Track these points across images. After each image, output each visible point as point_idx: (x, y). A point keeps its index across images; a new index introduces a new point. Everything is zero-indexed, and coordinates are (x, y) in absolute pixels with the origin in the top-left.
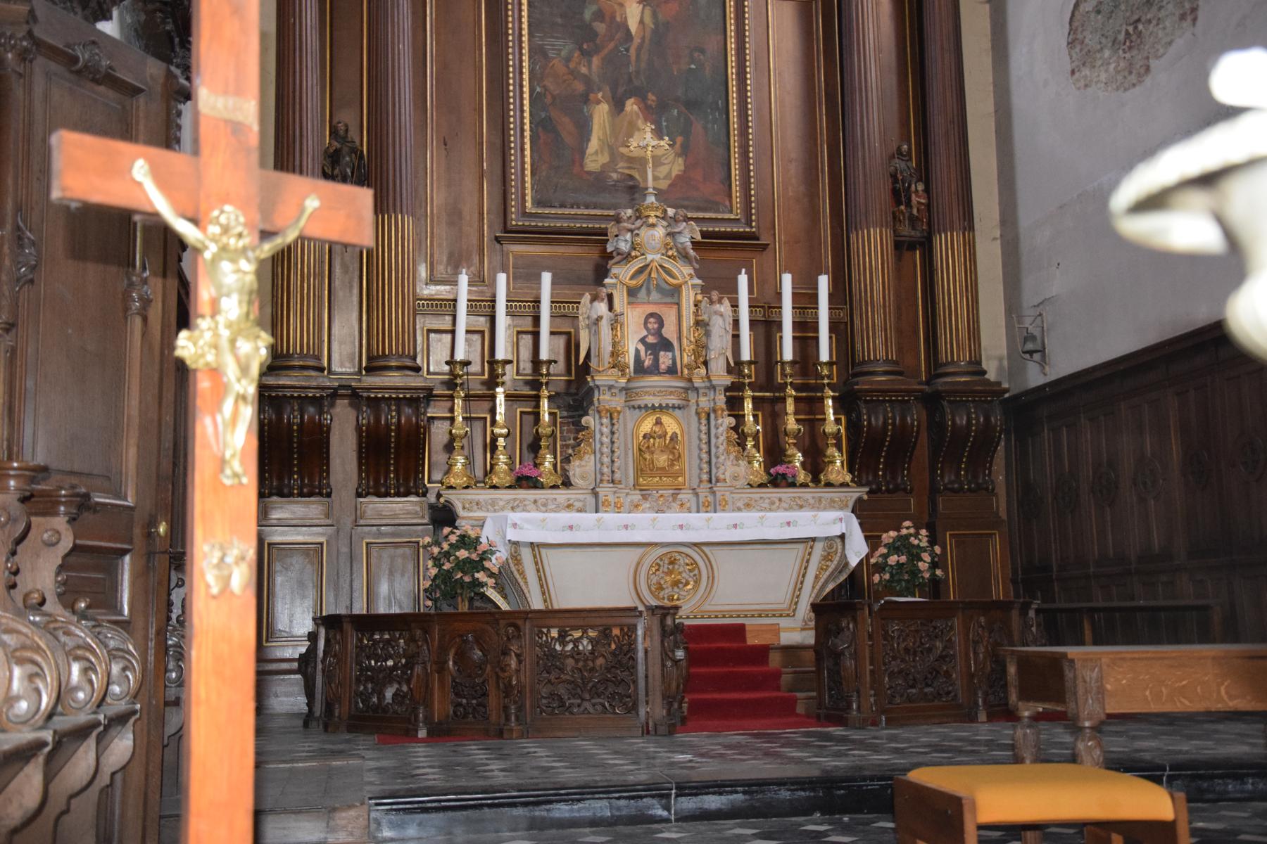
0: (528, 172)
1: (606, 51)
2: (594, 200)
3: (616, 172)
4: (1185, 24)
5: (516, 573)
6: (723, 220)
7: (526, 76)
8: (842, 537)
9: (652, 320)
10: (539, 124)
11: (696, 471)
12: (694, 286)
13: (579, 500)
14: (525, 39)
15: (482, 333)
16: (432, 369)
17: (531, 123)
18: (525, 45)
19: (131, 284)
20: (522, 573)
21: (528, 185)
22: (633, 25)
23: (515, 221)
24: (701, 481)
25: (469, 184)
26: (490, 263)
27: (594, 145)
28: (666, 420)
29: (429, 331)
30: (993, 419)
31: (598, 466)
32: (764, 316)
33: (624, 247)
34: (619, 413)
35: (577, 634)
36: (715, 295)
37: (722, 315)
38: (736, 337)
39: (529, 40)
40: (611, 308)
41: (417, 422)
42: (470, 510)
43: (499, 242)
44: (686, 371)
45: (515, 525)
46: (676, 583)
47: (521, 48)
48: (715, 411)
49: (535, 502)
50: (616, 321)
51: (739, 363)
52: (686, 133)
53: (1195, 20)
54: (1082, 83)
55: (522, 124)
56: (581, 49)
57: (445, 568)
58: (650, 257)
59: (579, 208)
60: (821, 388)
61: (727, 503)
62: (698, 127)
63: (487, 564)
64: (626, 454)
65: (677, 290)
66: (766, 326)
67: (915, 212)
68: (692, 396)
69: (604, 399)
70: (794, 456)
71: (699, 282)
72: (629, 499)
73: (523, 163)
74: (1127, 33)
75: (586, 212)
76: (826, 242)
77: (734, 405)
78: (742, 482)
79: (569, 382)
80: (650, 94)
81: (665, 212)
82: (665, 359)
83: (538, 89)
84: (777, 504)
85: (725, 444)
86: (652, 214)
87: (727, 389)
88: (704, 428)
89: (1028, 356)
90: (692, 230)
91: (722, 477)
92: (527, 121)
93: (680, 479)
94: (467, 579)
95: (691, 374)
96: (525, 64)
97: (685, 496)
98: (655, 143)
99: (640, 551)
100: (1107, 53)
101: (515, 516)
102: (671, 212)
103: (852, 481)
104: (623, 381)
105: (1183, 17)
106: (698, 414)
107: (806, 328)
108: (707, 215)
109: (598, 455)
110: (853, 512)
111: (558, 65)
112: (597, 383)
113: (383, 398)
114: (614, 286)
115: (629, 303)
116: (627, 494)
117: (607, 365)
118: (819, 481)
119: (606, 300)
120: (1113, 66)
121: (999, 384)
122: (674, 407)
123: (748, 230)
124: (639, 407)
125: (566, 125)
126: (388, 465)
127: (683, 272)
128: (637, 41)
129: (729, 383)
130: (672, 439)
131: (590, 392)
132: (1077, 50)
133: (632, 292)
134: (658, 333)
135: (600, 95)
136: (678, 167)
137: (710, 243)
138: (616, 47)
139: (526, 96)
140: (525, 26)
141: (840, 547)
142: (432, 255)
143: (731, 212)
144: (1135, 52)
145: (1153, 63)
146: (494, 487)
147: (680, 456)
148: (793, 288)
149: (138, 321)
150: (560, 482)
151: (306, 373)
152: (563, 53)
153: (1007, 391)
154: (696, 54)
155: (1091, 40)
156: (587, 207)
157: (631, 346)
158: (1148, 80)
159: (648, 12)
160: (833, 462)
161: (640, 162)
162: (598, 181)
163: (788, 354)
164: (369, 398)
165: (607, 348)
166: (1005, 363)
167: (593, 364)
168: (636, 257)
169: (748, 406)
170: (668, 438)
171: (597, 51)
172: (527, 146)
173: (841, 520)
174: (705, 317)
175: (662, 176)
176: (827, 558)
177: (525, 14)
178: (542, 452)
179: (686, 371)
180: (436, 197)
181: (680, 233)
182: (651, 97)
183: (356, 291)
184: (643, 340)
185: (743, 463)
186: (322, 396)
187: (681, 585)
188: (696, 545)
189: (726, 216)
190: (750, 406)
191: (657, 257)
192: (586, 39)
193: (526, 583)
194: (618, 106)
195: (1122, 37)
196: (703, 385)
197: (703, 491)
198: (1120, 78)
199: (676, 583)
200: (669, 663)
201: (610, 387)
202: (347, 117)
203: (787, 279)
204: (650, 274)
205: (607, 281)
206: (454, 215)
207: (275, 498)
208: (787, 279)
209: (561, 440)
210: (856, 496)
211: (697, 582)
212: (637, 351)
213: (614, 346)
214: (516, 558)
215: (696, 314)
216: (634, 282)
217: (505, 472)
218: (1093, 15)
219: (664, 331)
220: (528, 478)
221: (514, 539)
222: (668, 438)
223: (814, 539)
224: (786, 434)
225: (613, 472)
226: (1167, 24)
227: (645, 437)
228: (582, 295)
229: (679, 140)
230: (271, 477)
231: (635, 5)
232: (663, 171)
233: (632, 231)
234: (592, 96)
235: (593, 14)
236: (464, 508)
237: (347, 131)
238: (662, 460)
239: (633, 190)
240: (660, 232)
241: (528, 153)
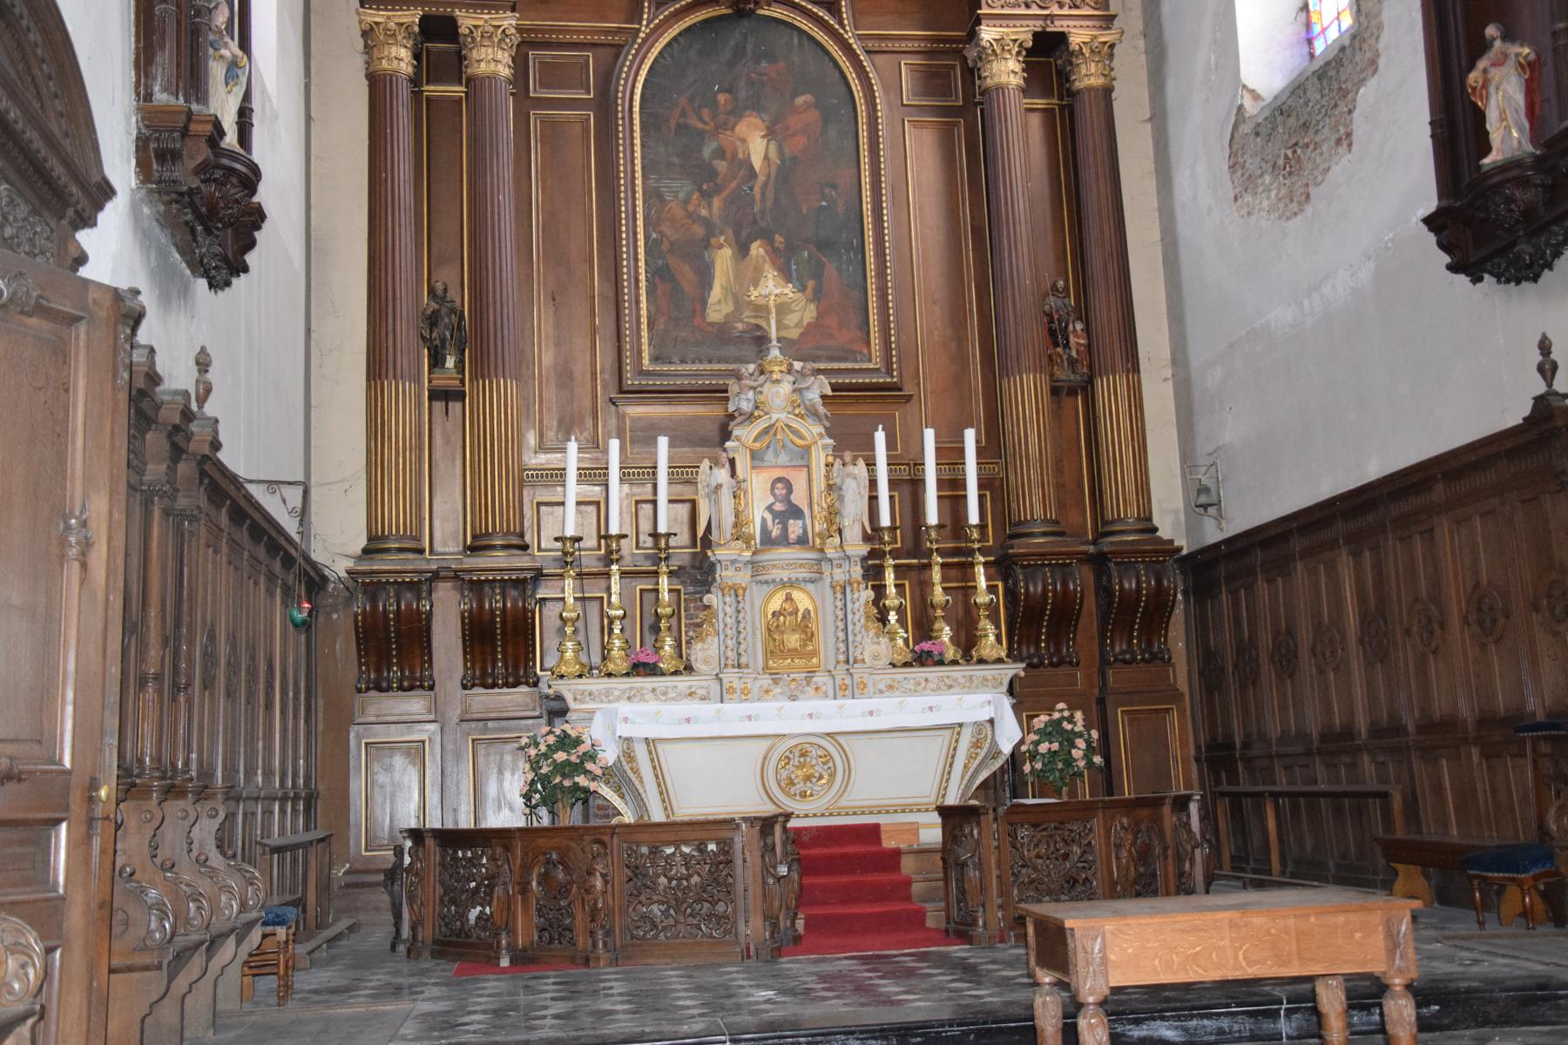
0: (644, 326)
1: (726, 193)
2: (718, 353)
3: (742, 321)
4: (1341, 150)
5: (629, 772)
6: (861, 370)
7: (640, 223)
8: (991, 721)
9: (779, 485)
10: (659, 274)
11: (832, 652)
12: (825, 447)
13: (702, 687)
14: (639, 182)
15: (598, 504)
16: (543, 546)
17: (646, 272)
18: (639, 189)
19: (68, 528)
20: (636, 772)
21: (645, 340)
22: (757, 162)
23: (630, 380)
24: (838, 662)
25: (580, 342)
26: (604, 426)
27: (716, 293)
28: (797, 595)
29: (539, 504)
30: (1166, 583)
31: (722, 648)
32: (910, 474)
33: (746, 406)
34: (745, 589)
35: (669, 850)
36: (848, 456)
37: (855, 478)
38: (873, 499)
39: (643, 183)
40: (733, 474)
41: (524, 606)
42: (582, 702)
43: (614, 403)
44: (818, 541)
45: (626, 720)
46: (808, 778)
47: (634, 192)
48: (850, 584)
49: (654, 690)
50: (739, 488)
51: (876, 528)
52: (818, 275)
53: (1350, 145)
54: (1245, 211)
55: (637, 274)
56: (700, 190)
57: (542, 771)
58: (775, 417)
59: (701, 362)
60: (971, 552)
61: (865, 686)
62: (831, 269)
63: (589, 766)
64: (754, 633)
65: (807, 450)
66: (908, 485)
67: (1074, 354)
68: (826, 567)
69: (725, 575)
70: (941, 630)
71: (830, 441)
72: (758, 684)
73: (639, 317)
74: (1286, 157)
75: (709, 367)
76: (976, 390)
77: (873, 574)
78: (884, 661)
79: (694, 555)
80: (777, 236)
81: (791, 365)
82: (795, 528)
83: (654, 235)
84: (923, 684)
85: (862, 620)
86: (776, 369)
87: (864, 559)
88: (839, 604)
89: (1201, 510)
90: (821, 385)
91: (860, 657)
92: (642, 270)
93: (814, 660)
94: (567, 783)
95: (823, 543)
96: (640, 209)
97: (821, 679)
98: (778, 291)
99: (765, 744)
100: (1267, 179)
101: (624, 708)
102: (798, 365)
103: (1008, 656)
104: (748, 554)
105: (1338, 142)
106: (833, 587)
107: (952, 488)
108: (843, 366)
109: (722, 637)
110: (1011, 691)
111: (675, 208)
112: (718, 557)
113: (487, 580)
114: (735, 450)
115: (753, 468)
116: (755, 679)
117: (729, 537)
118: (972, 657)
119: (727, 465)
120: (1273, 193)
121: (1172, 542)
122: (804, 580)
123: (889, 380)
124: (767, 582)
125: (686, 274)
126: (494, 653)
127: (813, 430)
128: (762, 178)
129: (865, 553)
130: (804, 617)
131: (712, 566)
132: (1239, 174)
133: (755, 456)
134: (787, 499)
135: (722, 239)
136: (810, 313)
137: (841, 394)
138: (739, 187)
139: (641, 243)
140: (638, 168)
141: (989, 733)
142: (541, 421)
143: (870, 361)
144: (1294, 179)
145: (1313, 191)
146: (609, 675)
147: (812, 635)
148: (936, 442)
149: (76, 565)
150: (682, 667)
151: (402, 556)
152: (681, 195)
153: (1180, 549)
154: (827, 191)
155: (1252, 164)
156: (710, 362)
157: (758, 514)
158: (1309, 209)
159: (773, 147)
160: (986, 636)
161: (761, 310)
162: (722, 335)
163: (932, 517)
164: (471, 581)
165: (728, 519)
166: (1182, 517)
167: (714, 537)
168: (760, 417)
169: (890, 577)
170: (800, 615)
171: (718, 190)
172: (643, 298)
173: (989, 702)
174: (837, 481)
175: (792, 325)
176: (977, 744)
177: (638, 155)
178: (662, 634)
179: (818, 541)
180: (547, 357)
181: (808, 388)
182: (779, 239)
183: (459, 463)
184: (770, 508)
185: (884, 640)
186: (420, 581)
187: (814, 780)
188: (828, 734)
189: (865, 366)
190: (892, 576)
191: (783, 416)
192: (705, 179)
193: (642, 782)
194: (743, 250)
195: (1281, 162)
196: (837, 555)
197: (840, 673)
198: (1281, 206)
199: (808, 778)
200: (771, 881)
201: (733, 562)
202: (447, 276)
203: (929, 435)
204: (775, 434)
205: (728, 444)
206: (565, 376)
207: (373, 693)
208: (929, 435)
209: (686, 618)
210: (1011, 673)
211: (832, 775)
212: (764, 520)
213: (737, 516)
214: (629, 755)
215: (827, 477)
216: (758, 445)
217: (621, 658)
218: (1252, 137)
219: (793, 497)
220: (645, 665)
221: (625, 735)
222: (800, 615)
223: (961, 725)
224: (933, 606)
225: (739, 655)
226: (1325, 148)
227: (774, 614)
228: (700, 460)
229: (811, 284)
230: (368, 670)
231: (759, 140)
232: (792, 319)
233: (754, 388)
234: (713, 241)
235: (713, 152)
236: (575, 699)
237: (445, 290)
238: (793, 640)
239: (760, 341)
240: (786, 388)
241: (644, 305)
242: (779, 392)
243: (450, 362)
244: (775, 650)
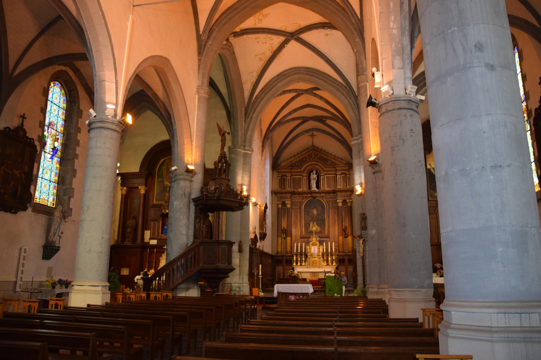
10: (305, 225)
22: (315, 214)
23: (302, 237)
33: (311, 240)
52: (321, 226)
69: (308, 257)
125: (308, 225)
194: (313, 223)
242: (314, 239)
243: (285, 235)
244: (313, 263)
